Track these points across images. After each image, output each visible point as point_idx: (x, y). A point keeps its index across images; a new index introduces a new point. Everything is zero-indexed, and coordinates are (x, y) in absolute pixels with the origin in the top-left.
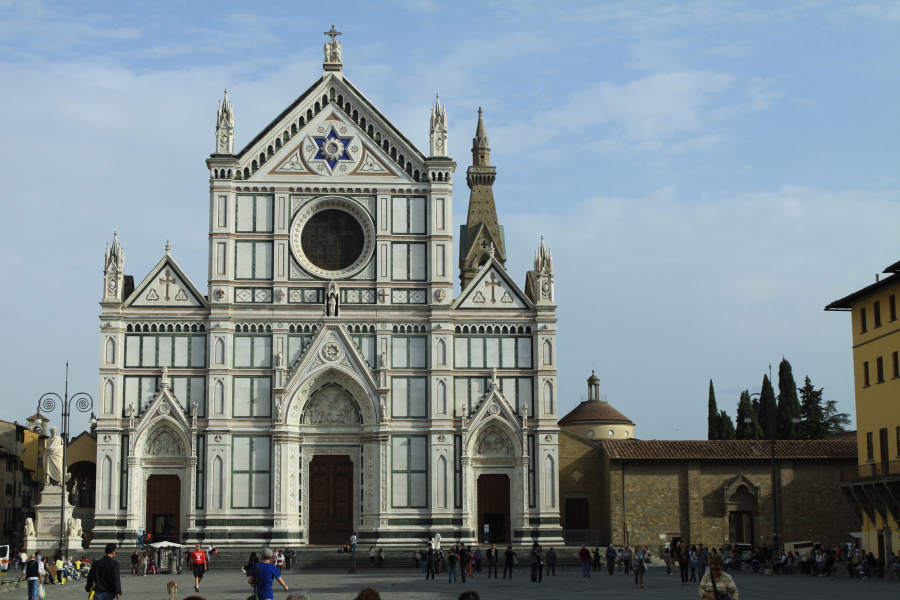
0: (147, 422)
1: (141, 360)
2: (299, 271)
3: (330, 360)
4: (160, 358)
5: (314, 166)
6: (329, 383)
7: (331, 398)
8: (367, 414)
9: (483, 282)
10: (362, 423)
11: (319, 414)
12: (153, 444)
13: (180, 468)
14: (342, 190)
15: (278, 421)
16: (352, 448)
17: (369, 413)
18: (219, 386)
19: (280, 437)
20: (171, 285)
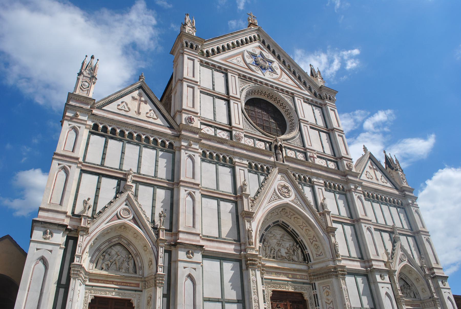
0: (103, 224)
1: (103, 159)
2: (250, 126)
3: (285, 197)
4: (125, 162)
5: (253, 67)
6: (278, 221)
7: (278, 237)
8: (314, 252)
9: (367, 167)
10: (311, 261)
11: (271, 250)
12: (102, 257)
13: (136, 291)
14: (272, 86)
15: (250, 245)
16: (304, 285)
17: (317, 251)
18: (189, 198)
19: (255, 261)
20: (143, 105)
